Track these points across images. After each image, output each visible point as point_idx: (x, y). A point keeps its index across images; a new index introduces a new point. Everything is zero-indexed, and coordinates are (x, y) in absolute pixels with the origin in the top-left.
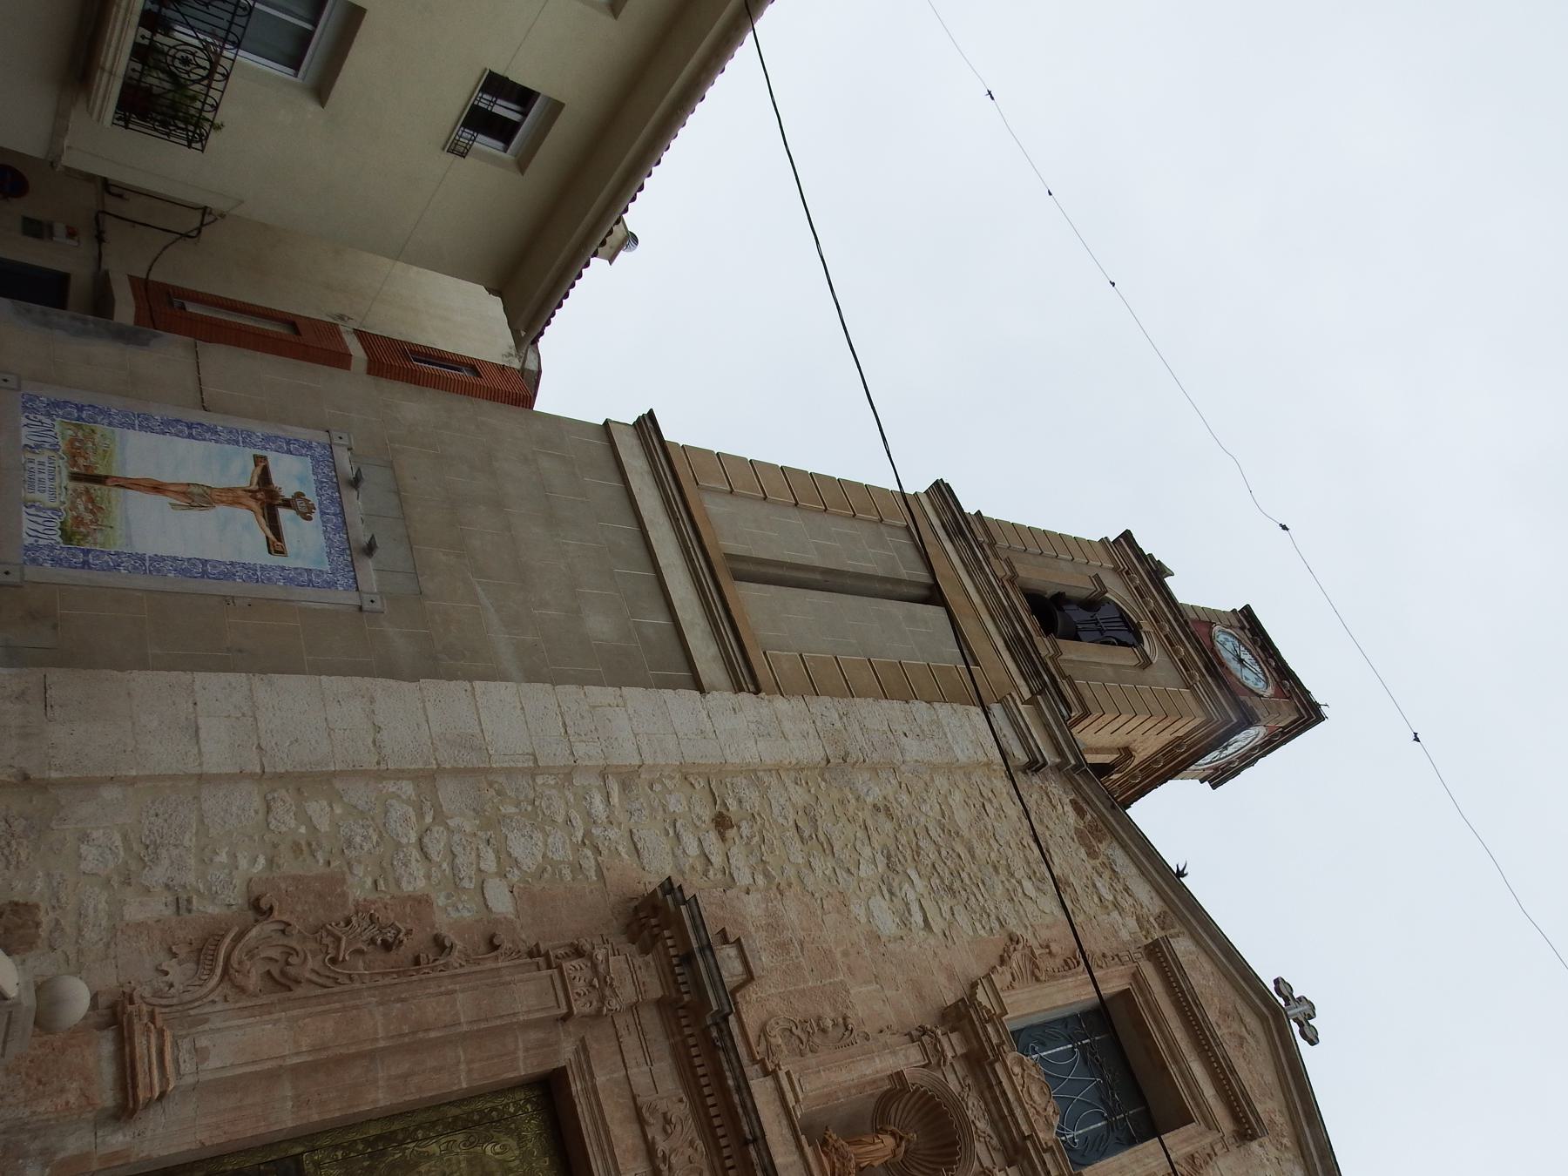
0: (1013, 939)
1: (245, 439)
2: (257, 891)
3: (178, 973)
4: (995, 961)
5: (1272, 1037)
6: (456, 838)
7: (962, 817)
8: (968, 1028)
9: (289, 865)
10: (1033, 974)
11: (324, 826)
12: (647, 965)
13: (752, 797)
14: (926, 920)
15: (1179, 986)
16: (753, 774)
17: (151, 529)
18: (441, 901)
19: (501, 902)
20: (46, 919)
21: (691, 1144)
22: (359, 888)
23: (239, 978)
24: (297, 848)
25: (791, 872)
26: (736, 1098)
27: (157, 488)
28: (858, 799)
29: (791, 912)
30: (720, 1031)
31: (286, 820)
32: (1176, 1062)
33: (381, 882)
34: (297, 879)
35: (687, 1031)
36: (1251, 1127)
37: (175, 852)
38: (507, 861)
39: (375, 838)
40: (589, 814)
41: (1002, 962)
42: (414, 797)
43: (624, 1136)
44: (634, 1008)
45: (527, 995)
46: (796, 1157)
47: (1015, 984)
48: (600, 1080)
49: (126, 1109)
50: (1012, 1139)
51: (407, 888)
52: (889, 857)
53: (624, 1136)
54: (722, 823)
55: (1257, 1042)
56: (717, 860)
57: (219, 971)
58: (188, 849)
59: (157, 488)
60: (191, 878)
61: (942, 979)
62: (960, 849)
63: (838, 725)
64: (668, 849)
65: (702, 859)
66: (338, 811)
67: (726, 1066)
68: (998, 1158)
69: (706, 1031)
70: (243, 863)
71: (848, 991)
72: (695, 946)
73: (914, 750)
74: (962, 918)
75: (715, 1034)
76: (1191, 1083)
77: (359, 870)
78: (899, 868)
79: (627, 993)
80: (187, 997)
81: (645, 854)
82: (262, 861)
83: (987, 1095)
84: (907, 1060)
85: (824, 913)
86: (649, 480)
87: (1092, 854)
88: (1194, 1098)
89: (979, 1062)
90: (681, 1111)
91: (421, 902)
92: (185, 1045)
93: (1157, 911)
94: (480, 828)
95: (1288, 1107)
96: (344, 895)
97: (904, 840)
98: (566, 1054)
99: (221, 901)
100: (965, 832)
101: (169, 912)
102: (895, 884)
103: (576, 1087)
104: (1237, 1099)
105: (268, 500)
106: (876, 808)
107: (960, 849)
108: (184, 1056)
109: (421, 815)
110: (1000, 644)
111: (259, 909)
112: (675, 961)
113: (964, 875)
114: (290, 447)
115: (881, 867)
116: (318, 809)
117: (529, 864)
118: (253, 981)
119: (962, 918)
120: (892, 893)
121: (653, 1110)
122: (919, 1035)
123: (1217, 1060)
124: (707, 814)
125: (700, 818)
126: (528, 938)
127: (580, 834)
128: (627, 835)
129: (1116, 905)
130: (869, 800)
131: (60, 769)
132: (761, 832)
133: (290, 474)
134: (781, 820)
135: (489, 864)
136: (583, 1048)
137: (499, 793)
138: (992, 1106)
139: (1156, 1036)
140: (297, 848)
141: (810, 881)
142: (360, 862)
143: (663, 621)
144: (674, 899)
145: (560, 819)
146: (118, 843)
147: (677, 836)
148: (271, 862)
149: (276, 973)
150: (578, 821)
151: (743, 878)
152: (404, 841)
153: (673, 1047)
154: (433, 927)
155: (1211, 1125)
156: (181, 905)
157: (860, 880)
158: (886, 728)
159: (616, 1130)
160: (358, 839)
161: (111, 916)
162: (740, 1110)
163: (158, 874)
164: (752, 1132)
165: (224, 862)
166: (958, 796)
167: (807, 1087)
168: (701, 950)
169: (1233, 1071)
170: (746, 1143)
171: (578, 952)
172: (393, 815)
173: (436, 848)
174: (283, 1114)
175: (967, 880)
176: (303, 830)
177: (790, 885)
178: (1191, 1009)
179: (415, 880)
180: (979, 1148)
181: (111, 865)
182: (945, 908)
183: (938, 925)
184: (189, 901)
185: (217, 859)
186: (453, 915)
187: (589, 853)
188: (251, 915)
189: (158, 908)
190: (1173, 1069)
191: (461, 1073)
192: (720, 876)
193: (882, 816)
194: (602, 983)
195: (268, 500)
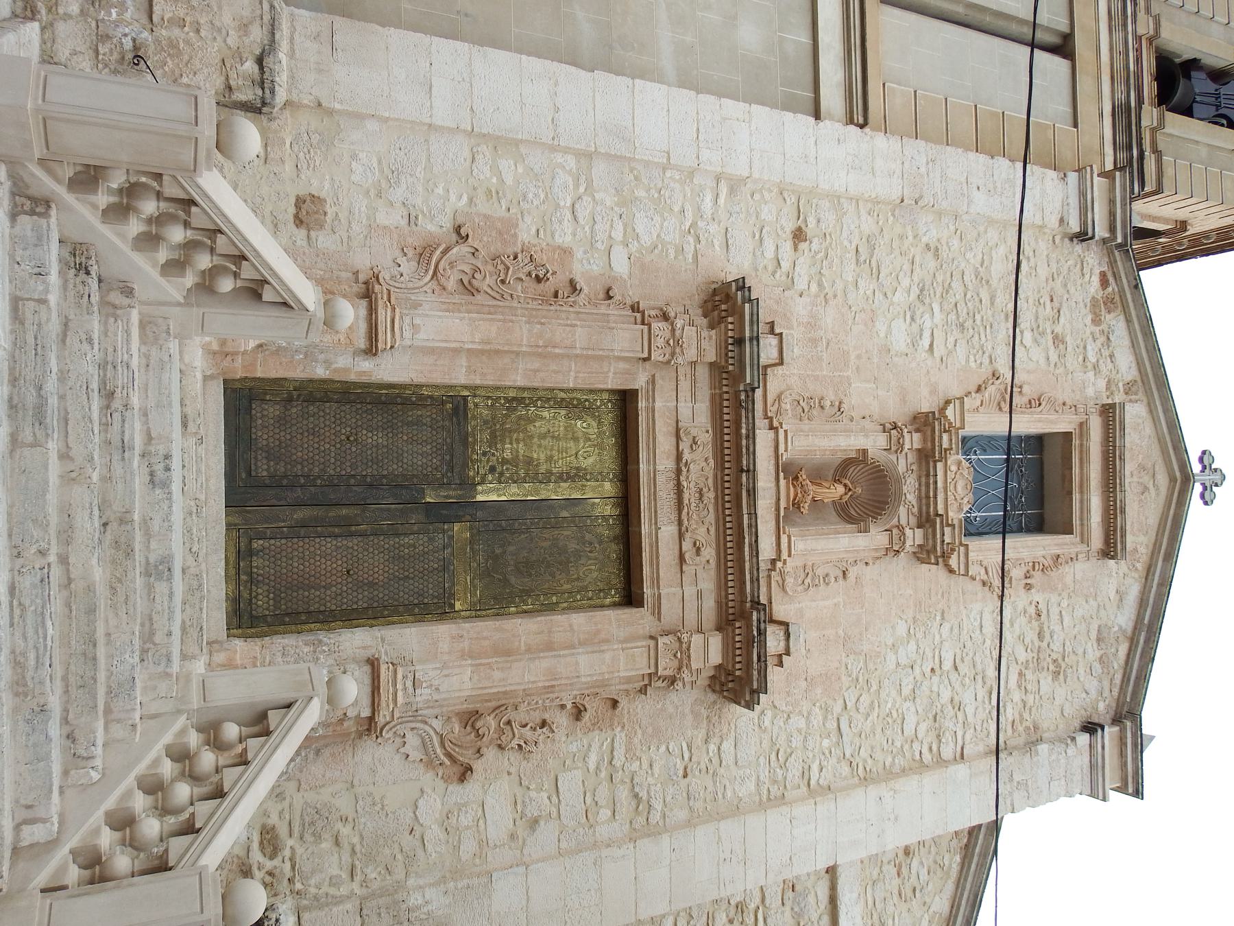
2: (460, 220)
3: (408, 267)
4: (973, 388)
5: (1172, 494)
6: (598, 209)
8: (929, 433)
9: (483, 207)
10: (999, 404)
11: (509, 181)
12: (710, 338)
13: (829, 218)
14: (931, 345)
15: (1114, 442)
16: (836, 199)
18: (579, 254)
19: (621, 265)
20: (331, 211)
21: (706, 460)
22: (525, 234)
23: (443, 280)
24: (489, 193)
25: (839, 286)
26: (744, 442)
28: (915, 237)
29: (829, 318)
30: (747, 396)
31: (483, 170)
32: (1081, 492)
33: (541, 232)
34: (487, 217)
35: (725, 389)
36: (1116, 551)
37: (410, 180)
38: (631, 234)
39: (542, 196)
40: (699, 209)
41: (979, 390)
42: (574, 170)
44: (693, 364)
45: (624, 338)
46: (773, 485)
47: (981, 409)
48: (658, 404)
49: (371, 350)
50: (928, 513)
51: (559, 240)
52: (922, 291)
53: (665, 444)
54: (799, 236)
55: (1158, 495)
56: (785, 265)
57: (431, 272)
58: (418, 179)
60: (419, 201)
61: (925, 392)
62: (985, 296)
63: (923, 170)
64: (751, 249)
65: (775, 263)
66: (520, 170)
67: (744, 420)
68: (913, 521)
69: (737, 393)
70: (453, 198)
71: (850, 384)
72: (747, 334)
74: (961, 351)
75: (743, 397)
77: (528, 220)
78: (927, 301)
79: (691, 354)
80: (411, 285)
81: (732, 249)
82: (465, 198)
83: (923, 479)
85: (854, 324)
87: (1096, 321)
88: (1081, 519)
89: (927, 457)
90: (706, 438)
91: (566, 252)
92: (407, 320)
93: (1129, 378)
94: (617, 204)
95: (1155, 544)
96: (515, 235)
97: (940, 278)
98: (639, 382)
99: (437, 226)
100: (994, 283)
101: (404, 222)
102: (918, 313)
103: (642, 404)
104: (1115, 531)
106: (928, 247)
107: (985, 296)
108: (406, 327)
109: (577, 186)
111: (460, 235)
112: (730, 341)
113: (978, 317)
115: (913, 296)
116: (506, 165)
117: (646, 240)
118: (451, 284)
119: (961, 351)
120: (913, 319)
121: (687, 433)
123: (1115, 501)
124: (790, 226)
125: (782, 229)
126: (633, 295)
127: (688, 224)
128: (723, 231)
129: (1096, 367)
130: (925, 240)
131: (341, 102)
132: (827, 249)
134: (846, 243)
135: (618, 234)
136: (653, 381)
137: (636, 178)
138: (923, 488)
139: (1076, 470)
140: (489, 193)
141: (852, 297)
142: (529, 213)
143: (805, 39)
144: (743, 296)
145: (676, 209)
146: (375, 165)
147: (761, 239)
148: (471, 200)
149: (466, 283)
150: (689, 215)
151: (801, 284)
152: (562, 204)
153: (713, 397)
154: (571, 272)
155: (1085, 539)
156: (411, 220)
157: (892, 304)
158: (963, 180)
159: (660, 438)
160: (531, 196)
161: (368, 218)
162: (744, 450)
163: (398, 194)
164: (748, 465)
167: (796, 443)
168: (751, 339)
169: (1123, 511)
170: (742, 471)
171: (665, 317)
172: (558, 182)
173: (583, 213)
174: (459, 375)
175: (978, 322)
176: (494, 180)
177: (835, 296)
178: (1114, 461)
179: (564, 235)
180: (902, 511)
181: (370, 181)
182: (951, 340)
183: (939, 350)
184: (416, 218)
185: (436, 191)
186: (585, 267)
187: (691, 240)
188: (454, 237)
190: (1076, 496)
191: (571, 377)
192: (784, 278)
193: (930, 254)
194: (675, 343)
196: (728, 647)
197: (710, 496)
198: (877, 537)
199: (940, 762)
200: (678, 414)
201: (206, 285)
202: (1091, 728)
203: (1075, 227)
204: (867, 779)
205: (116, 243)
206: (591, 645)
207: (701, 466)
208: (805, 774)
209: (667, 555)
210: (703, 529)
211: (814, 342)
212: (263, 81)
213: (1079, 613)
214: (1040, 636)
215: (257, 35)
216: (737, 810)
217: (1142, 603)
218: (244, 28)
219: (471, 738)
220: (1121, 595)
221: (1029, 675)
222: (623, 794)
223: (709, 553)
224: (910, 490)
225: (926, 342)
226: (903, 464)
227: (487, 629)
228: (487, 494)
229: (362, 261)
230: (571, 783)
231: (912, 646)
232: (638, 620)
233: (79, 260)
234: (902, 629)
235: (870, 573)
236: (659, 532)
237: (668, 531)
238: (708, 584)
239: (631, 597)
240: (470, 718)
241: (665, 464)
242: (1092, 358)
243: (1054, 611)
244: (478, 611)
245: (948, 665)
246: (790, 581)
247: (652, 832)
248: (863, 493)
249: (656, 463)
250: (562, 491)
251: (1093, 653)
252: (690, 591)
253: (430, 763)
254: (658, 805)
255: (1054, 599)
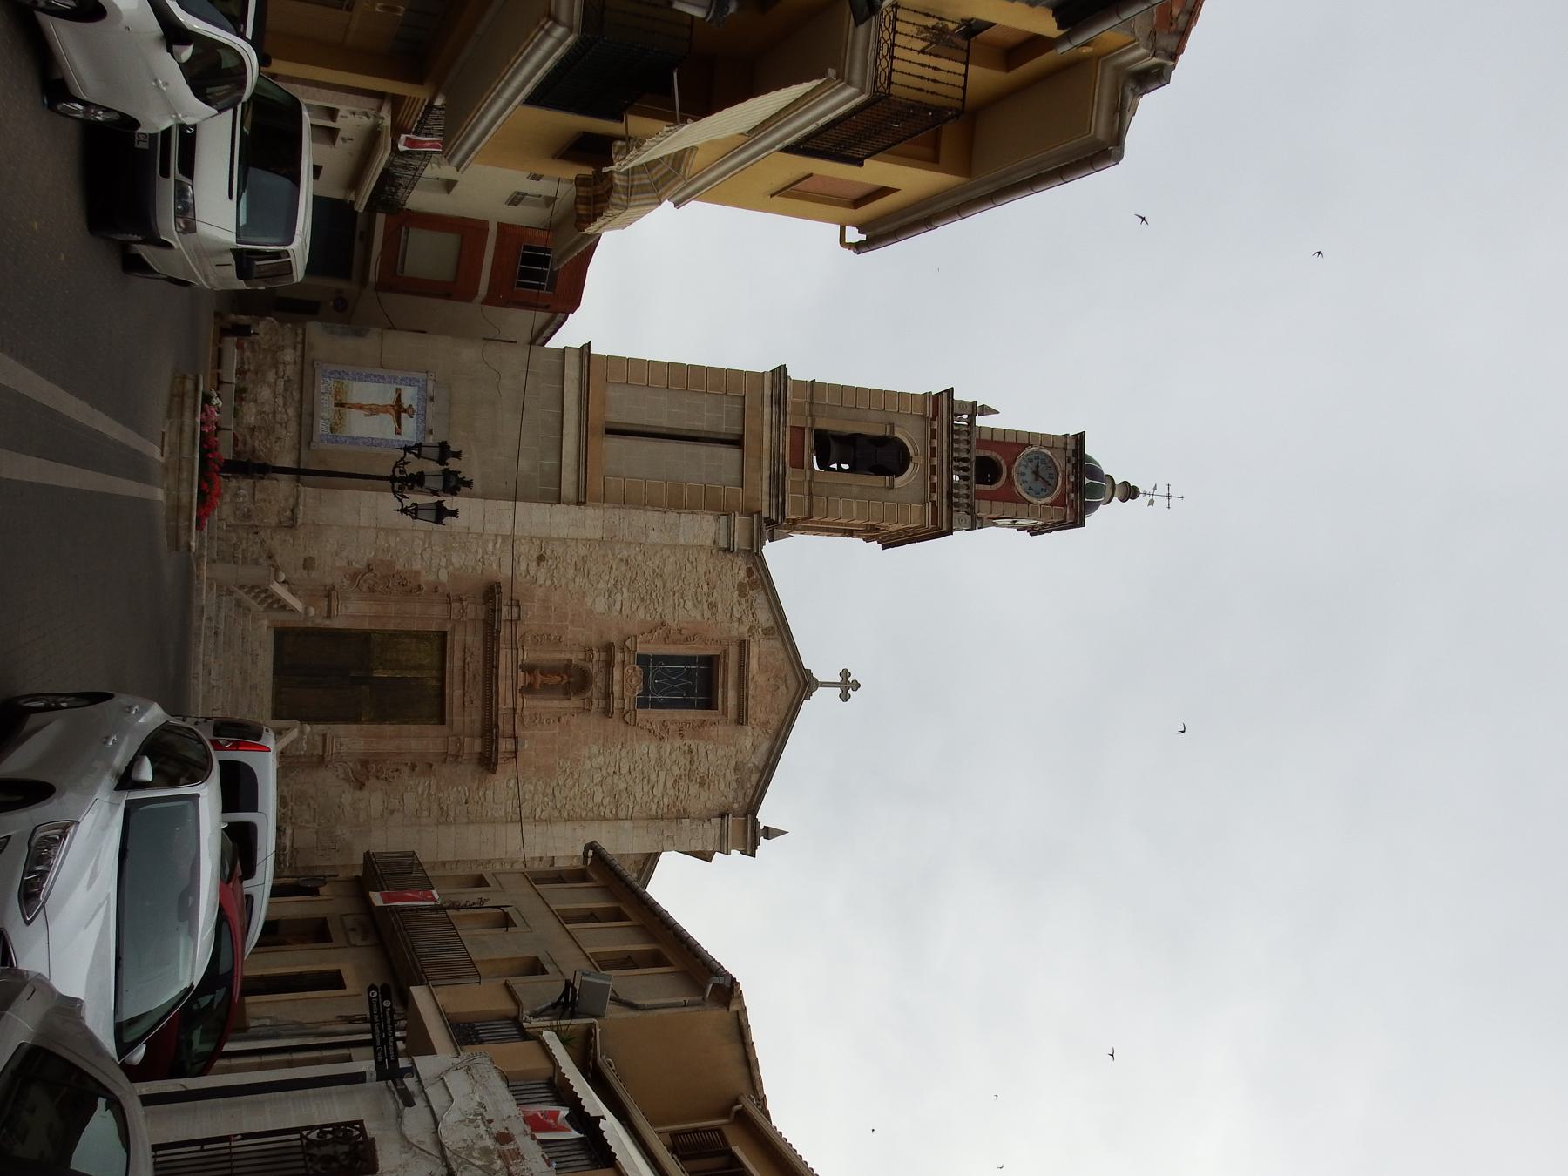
0: (663, 624)
1: (392, 380)
3: (346, 583)
7: (668, 568)
16: (564, 541)
17: (361, 426)
19: (443, 577)
25: (564, 582)
27: (361, 407)
43: (458, 654)
44: (474, 620)
45: (437, 610)
49: (329, 617)
53: (458, 654)
54: (541, 559)
59: (361, 407)
62: (659, 583)
73: (654, 537)
74: (641, 613)
76: (725, 697)
79: (471, 616)
84: (576, 657)
86: (576, 383)
87: (742, 594)
89: (609, 665)
90: (479, 652)
91: (417, 573)
93: (768, 625)
98: (448, 627)
99: (359, 565)
105: (398, 409)
107: (659, 583)
110: (766, 474)
111: (369, 568)
114: (410, 382)
118: (365, 589)
122: (588, 650)
124: (536, 555)
133: (409, 396)
136: (453, 628)
141: (571, 586)
143: (555, 462)
151: (541, 581)
155: (724, 713)
163: (344, 554)
165: (363, 554)
166: (672, 559)
171: (461, 600)
173: (426, 556)
174: (366, 626)
179: (417, 566)
182: (634, 607)
186: (426, 578)
189: (344, 563)
190: (720, 690)
191: (415, 626)
195: (398, 409)
196: (483, 746)
197: (479, 678)
198: (575, 702)
199: (617, 819)
200: (465, 642)
201: (270, 606)
202: (722, 816)
203: (723, 543)
204: (570, 820)
205: (248, 599)
206: (418, 739)
207: (476, 664)
208: (533, 811)
209: (457, 702)
210: (476, 693)
211: (547, 608)
212: (293, 518)
213: (721, 753)
214: (691, 763)
215: (292, 501)
216: (493, 822)
217: (771, 751)
218: (287, 500)
219: (363, 773)
220: (755, 747)
221: (682, 783)
222: (435, 806)
223: (478, 703)
224: (599, 681)
225: (618, 607)
226: (594, 669)
227: (373, 728)
228: (379, 674)
229: (328, 581)
230: (410, 798)
231: (601, 759)
232: (444, 729)
233: (239, 604)
234: (595, 749)
235: (574, 720)
236: (454, 693)
237: (458, 692)
238: (477, 716)
239: (443, 722)
240: (365, 764)
241: (458, 663)
242: (737, 614)
243: (702, 751)
244: (371, 721)
245: (624, 771)
246: (527, 720)
247: (446, 822)
248: (574, 681)
249: (454, 662)
250: (413, 674)
251: (731, 775)
252: (467, 719)
253: (347, 780)
254: (452, 814)
255: (701, 744)
